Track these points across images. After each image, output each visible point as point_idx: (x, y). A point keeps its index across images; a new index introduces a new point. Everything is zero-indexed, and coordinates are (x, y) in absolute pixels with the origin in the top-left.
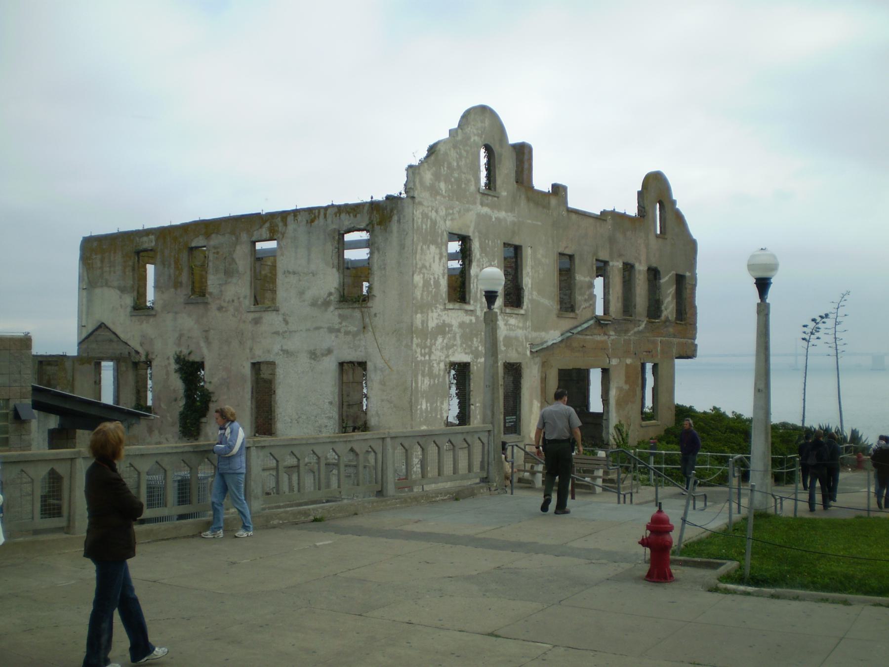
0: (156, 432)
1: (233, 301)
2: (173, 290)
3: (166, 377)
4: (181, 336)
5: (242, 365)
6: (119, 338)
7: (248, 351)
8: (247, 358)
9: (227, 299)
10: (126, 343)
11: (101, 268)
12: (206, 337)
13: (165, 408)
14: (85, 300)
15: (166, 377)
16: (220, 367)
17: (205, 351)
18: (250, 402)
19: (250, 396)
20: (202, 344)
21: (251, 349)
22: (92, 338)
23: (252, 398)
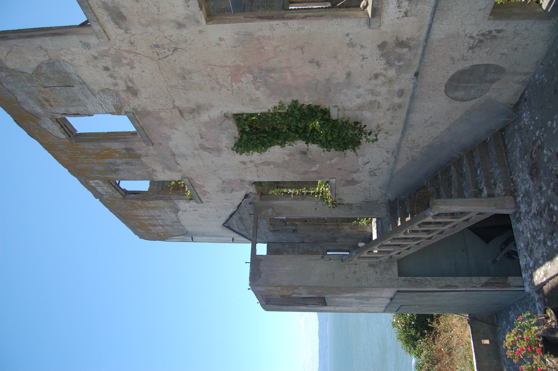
0: (354, 176)
1: (106, 69)
2: (143, 159)
3: (272, 166)
4: (204, 148)
5: (218, 44)
6: (234, 212)
7: (185, 31)
8: (201, 32)
9: (110, 80)
10: (239, 206)
11: (162, 226)
12: (191, 113)
13: (318, 165)
14: (205, 238)
15: (272, 166)
16: (235, 87)
17: (215, 113)
18: (290, 22)
19: (277, 22)
20: (204, 117)
21: (180, 26)
22: (244, 233)
23: (283, 18)
